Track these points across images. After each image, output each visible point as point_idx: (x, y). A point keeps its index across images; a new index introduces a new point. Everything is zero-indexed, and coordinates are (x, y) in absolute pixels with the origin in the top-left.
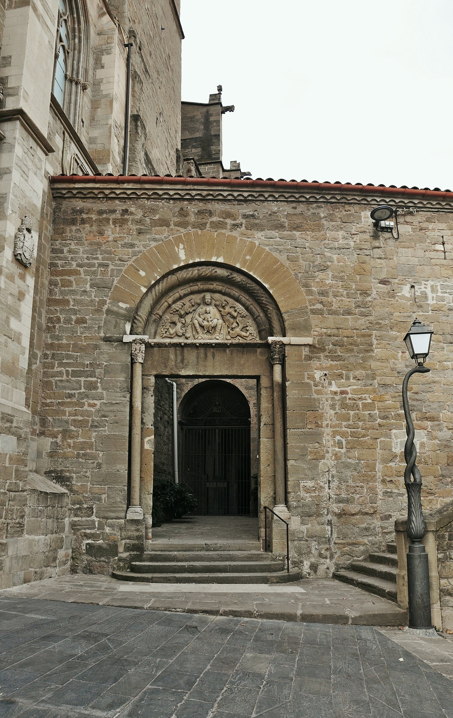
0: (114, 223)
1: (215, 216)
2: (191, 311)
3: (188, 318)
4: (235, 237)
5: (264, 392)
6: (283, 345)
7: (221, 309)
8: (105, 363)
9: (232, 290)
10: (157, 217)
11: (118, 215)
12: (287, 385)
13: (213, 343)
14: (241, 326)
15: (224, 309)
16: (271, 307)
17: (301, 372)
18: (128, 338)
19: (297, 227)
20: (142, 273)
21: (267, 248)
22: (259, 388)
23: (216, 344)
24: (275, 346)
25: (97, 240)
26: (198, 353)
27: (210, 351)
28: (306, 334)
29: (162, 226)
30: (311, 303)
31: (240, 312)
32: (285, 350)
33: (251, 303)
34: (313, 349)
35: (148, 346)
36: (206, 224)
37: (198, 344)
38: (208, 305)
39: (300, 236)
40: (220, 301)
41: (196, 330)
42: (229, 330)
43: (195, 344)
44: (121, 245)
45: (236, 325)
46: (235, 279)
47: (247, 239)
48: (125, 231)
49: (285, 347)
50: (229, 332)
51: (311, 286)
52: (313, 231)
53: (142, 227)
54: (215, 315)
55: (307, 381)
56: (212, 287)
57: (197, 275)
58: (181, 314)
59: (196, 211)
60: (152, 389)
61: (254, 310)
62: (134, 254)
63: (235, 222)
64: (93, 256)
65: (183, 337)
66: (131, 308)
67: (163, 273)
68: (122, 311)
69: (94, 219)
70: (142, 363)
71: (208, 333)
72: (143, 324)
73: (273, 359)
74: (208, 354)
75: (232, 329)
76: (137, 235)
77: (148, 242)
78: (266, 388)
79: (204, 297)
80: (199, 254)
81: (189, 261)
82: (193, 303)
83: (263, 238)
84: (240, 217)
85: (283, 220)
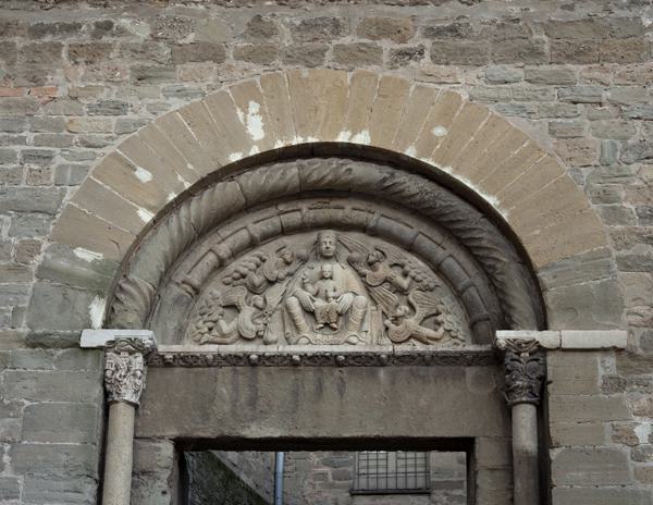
0: (74, 54)
1: (349, 34)
2: (282, 275)
3: (273, 296)
4: (402, 81)
5: (485, 481)
6: (541, 351)
7: (365, 270)
8: (27, 403)
9: (397, 220)
10: (191, 37)
11: (85, 38)
12: (553, 458)
13: (340, 354)
14: (421, 312)
15: (375, 270)
16: (504, 258)
17: (593, 421)
18: (94, 337)
19: (578, 53)
20: (144, 175)
21: (492, 108)
22: (472, 473)
23: (347, 356)
24: (515, 357)
25: (26, 95)
27: (332, 374)
28: (607, 323)
29: (203, 61)
30: (620, 242)
31: (419, 277)
32: (545, 364)
33: (448, 251)
34: (627, 360)
35: (153, 359)
36: (322, 52)
37: (296, 358)
38: (327, 258)
39: (584, 74)
40: (363, 249)
42: (388, 322)
43: (290, 356)
44: (89, 106)
45: (407, 309)
46: (402, 187)
47: (437, 86)
48: (100, 73)
49: (545, 356)
50: (387, 329)
51: (617, 199)
52: (622, 60)
53: (149, 64)
54: (348, 284)
55: (610, 444)
56: (339, 214)
57: (296, 181)
58: (254, 285)
59: (298, 23)
60: (165, 475)
61: (457, 268)
62: (124, 129)
63: (403, 46)
64: (11, 135)
65: (258, 341)
66: (107, 260)
67: (203, 172)
68: (83, 271)
69: (19, 46)
70: (136, 406)
71: (327, 331)
72: (142, 303)
73: (510, 390)
74: (327, 383)
75: (396, 320)
76: (136, 84)
77: (162, 99)
78: (492, 470)
79: (317, 243)
80: (301, 126)
81: (274, 142)
82: (288, 258)
83: (482, 82)
84: (418, 34)
85: (536, 37)
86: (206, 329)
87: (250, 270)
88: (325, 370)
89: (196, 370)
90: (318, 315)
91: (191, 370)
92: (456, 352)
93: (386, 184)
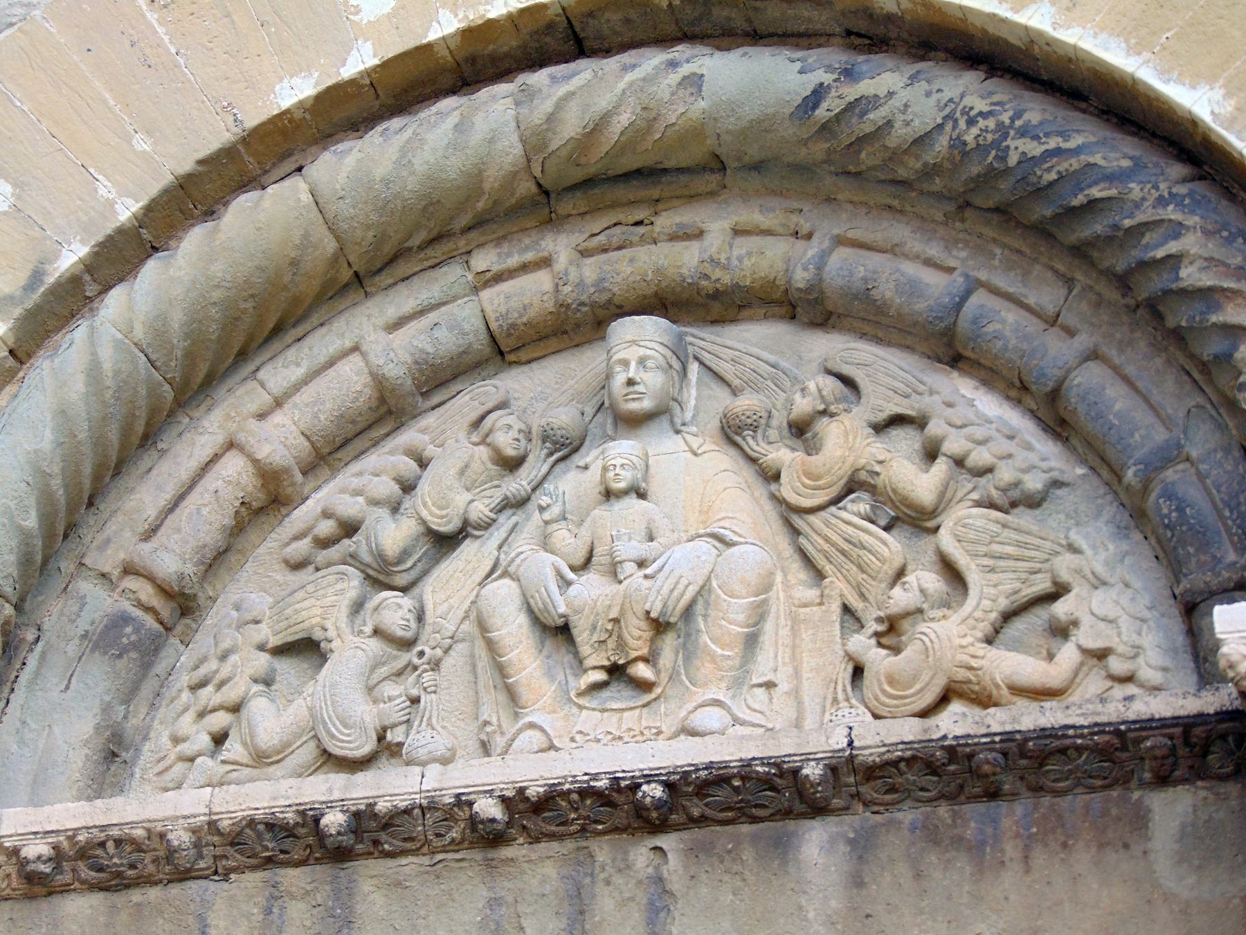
7: (782, 455)
9: (893, 250)
13: (649, 778)
15: (812, 448)
26: (494, 903)
27: (626, 868)
31: (979, 457)
37: (489, 808)
38: (633, 422)
41: (501, 670)
43: (462, 802)
57: (510, 149)
58: (380, 556)
71: (618, 697)
81: (430, 18)
86: (205, 740)
87: (375, 503)
88: (602, 850)
89: (136, 896)
90: (582, 635)
91: (119, 899)
92: (1097, 727)
93: (822, 113)
